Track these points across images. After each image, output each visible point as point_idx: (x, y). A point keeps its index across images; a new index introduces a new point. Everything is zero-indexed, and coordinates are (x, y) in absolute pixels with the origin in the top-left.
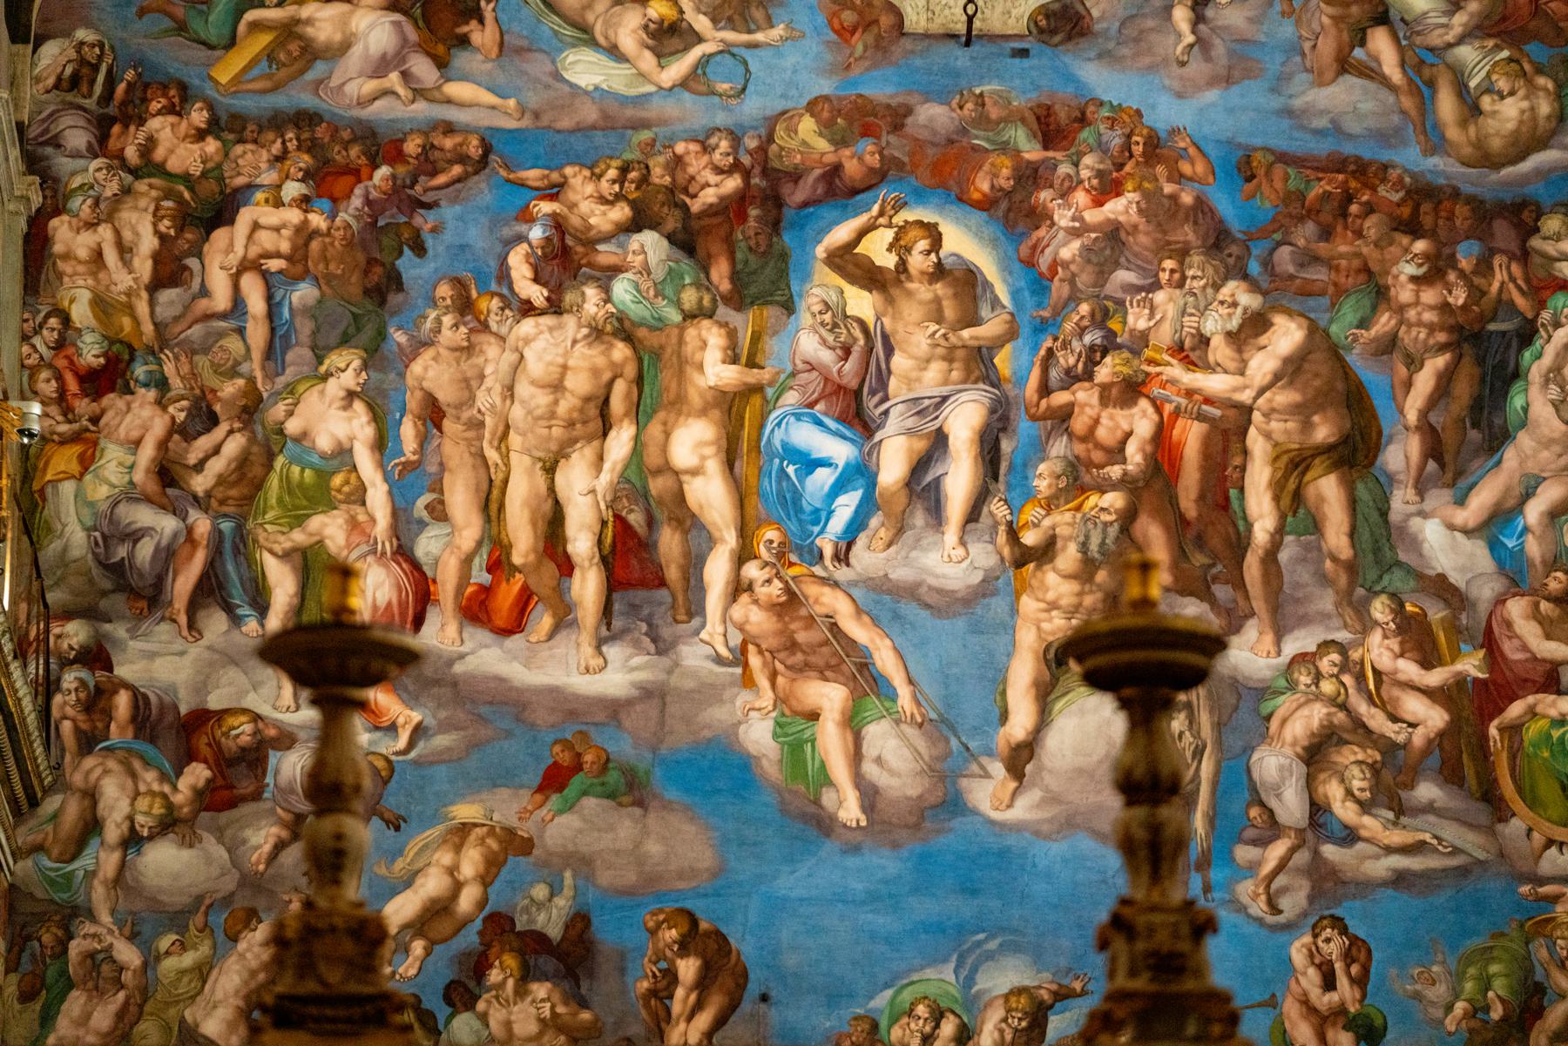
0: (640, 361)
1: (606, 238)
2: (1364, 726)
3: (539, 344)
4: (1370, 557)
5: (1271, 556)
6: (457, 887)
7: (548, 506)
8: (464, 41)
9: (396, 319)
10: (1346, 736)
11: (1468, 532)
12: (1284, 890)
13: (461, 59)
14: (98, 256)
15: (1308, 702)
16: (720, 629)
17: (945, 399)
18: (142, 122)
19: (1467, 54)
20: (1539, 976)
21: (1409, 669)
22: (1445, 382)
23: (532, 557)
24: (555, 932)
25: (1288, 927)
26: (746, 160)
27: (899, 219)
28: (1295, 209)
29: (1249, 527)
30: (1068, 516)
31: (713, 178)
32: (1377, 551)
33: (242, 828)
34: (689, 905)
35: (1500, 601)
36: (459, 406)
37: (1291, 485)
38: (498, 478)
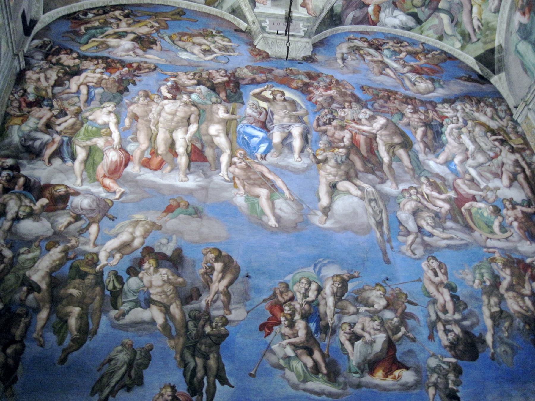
0: (199, 111)
1: (190, 86)
2: (427, 207)
3: (169, 105)
4: (417, 168)
5: (390, 166)
7: (170, 141)
8: (152, 48)
9: (126, 97)
10: (423, 209)
11: (441, 164)
12: (415, 249)
13: (149, 51)
14: (39, 79)
15: (409, 201)
16: (226, 173)
17: (290, 126)
18: (58, 55)
20: (497, 273)
21: (435, 194)
22: (425, 134)
23: (164, 152)
24: (169, 253)
25: (418, 259)
26: (229, 75)
27: (273, 89)
28: (376, 97)
29: (382, 159)
30: (330, 153)
31: (220, 77)
33: (57, 218)
34: (218, 247)
35: (455, 180)
36: (143, 117)
37: (391, 150)
38: (154, 133)
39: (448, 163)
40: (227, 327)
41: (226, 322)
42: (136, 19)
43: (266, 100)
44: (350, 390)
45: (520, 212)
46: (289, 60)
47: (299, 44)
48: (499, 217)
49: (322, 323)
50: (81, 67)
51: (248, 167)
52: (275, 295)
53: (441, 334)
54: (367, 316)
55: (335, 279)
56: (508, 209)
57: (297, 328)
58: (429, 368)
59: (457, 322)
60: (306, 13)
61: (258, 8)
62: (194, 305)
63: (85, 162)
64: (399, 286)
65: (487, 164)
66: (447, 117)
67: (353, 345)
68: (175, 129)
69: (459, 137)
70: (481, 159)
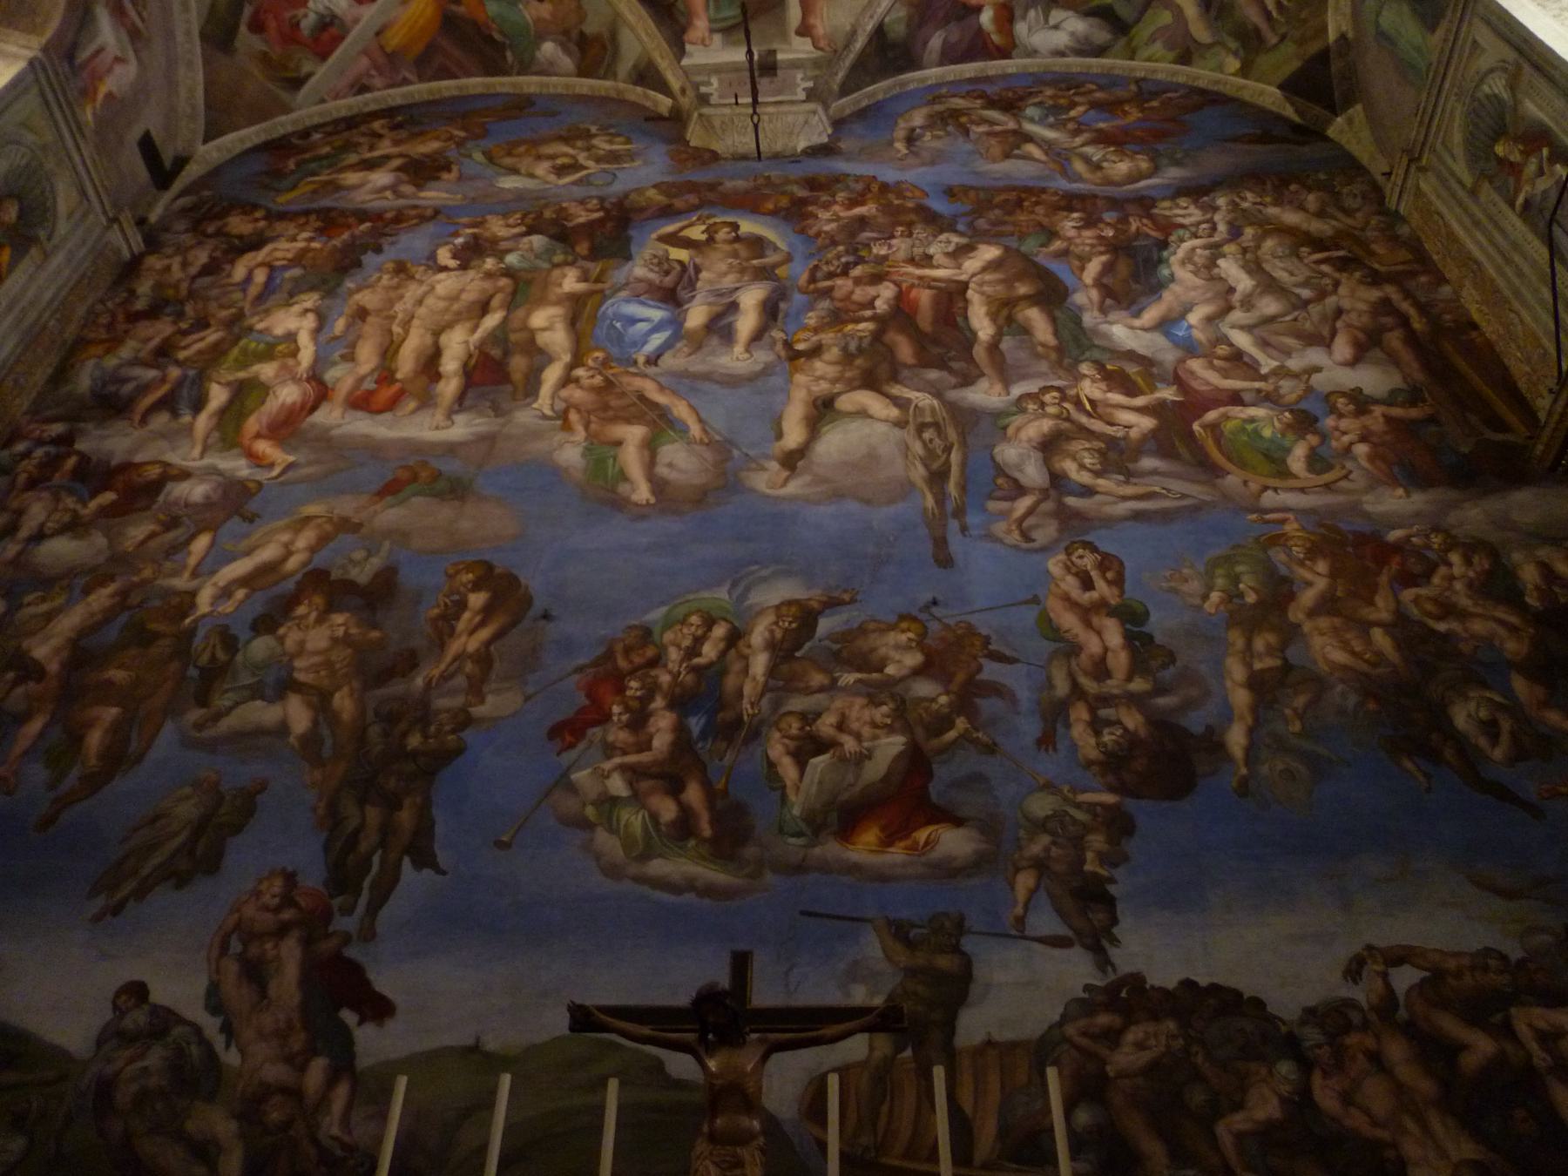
3: (449, 282)
5: (994, 347)
6: (289, 554)
8: (438, 178)
12: (1037, 526)
14: (168, 268)
16: (548, 402)
17: (737, 289)
19: (1089, 150)
20: (1283, 571)
21: (1116, 397)
22: (1108, 269)
27: (712, 221)
30: (831, 335)
32: (1076, 340)
34: (487, 557)
35: (1182, 361)
36: (378, 312)
37: (1005, 312)
39: (1164, 325)
40: (468, 735)
41: (464, 720)
42: (416, 130)
43: (688, 244)
44: (769, 877)
45: (1381, 420)
46: (769, 158)
47: (790, 118)
48: (1309, 437)
49: (726, 716)
50: (268, 234)
51: (609, 385)
52: (609, 655)
53: (1079, 731)
54: (858, 694)
55: (784, 610)
56: (1341, 416)
57: (652, 730)
58: (1027, 819)
59: (1134, 700)
60: (812, 48)
61: (691, 55)
62: (396, 688)
63: (222, 412)
64: (963, 618)
65: (1288, 318)
66: (1182, 226)
67: (802, 765)
68: (449, 326)
69: (1212, 263)
70: (1270, 306)
